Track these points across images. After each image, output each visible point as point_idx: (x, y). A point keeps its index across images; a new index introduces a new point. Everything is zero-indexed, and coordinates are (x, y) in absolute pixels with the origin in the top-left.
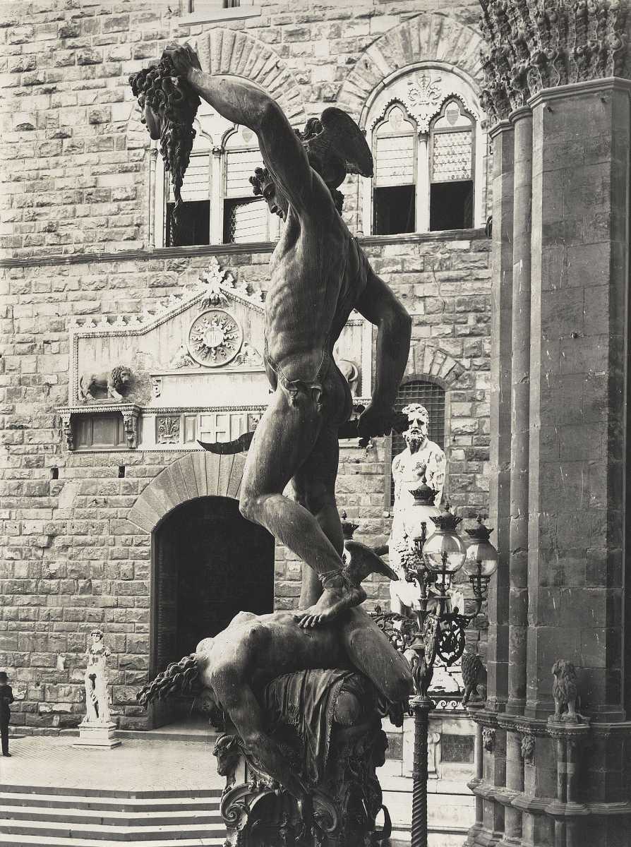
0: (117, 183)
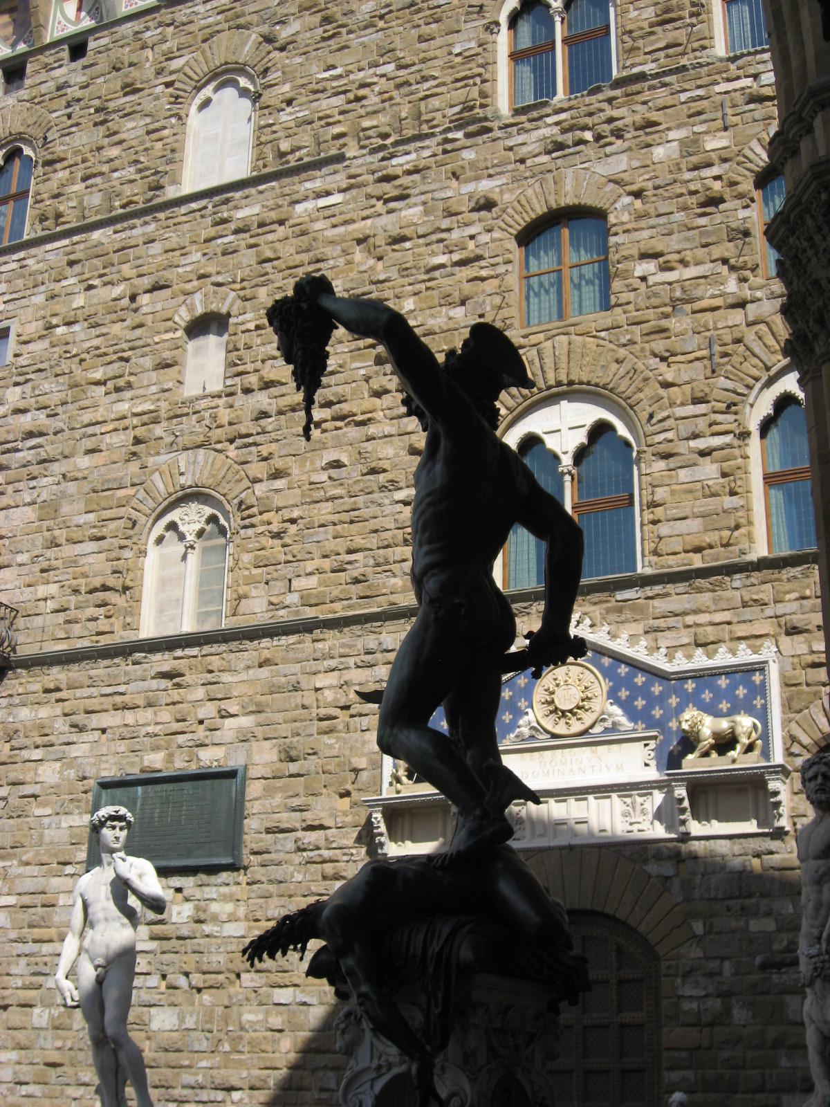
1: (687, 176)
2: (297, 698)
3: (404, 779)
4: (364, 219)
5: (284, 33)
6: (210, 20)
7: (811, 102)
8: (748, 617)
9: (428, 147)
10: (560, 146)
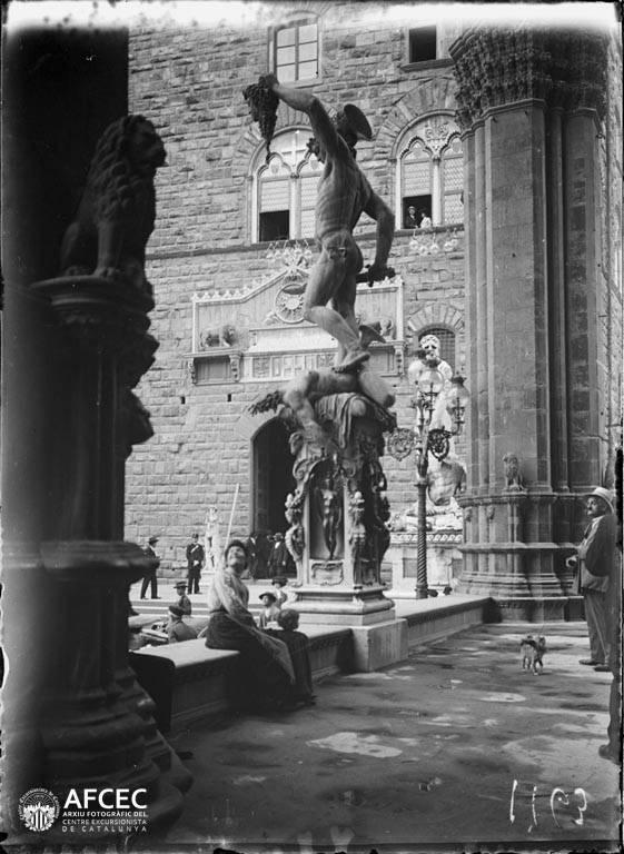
0: (227, 201)
3: (207, 346)
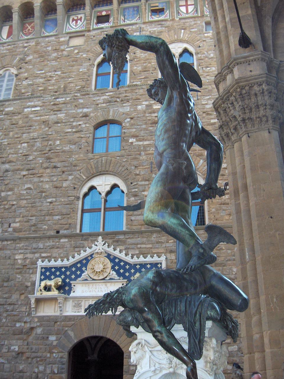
1: (147, 115)
2: (9, 262)
3: (43, 290)
4: (46, 115)
5: (28, 59)
6: (5, 52)
7: (234, 62)
8: (157, 247)
9: (69, 97)
10: (110, 102)
